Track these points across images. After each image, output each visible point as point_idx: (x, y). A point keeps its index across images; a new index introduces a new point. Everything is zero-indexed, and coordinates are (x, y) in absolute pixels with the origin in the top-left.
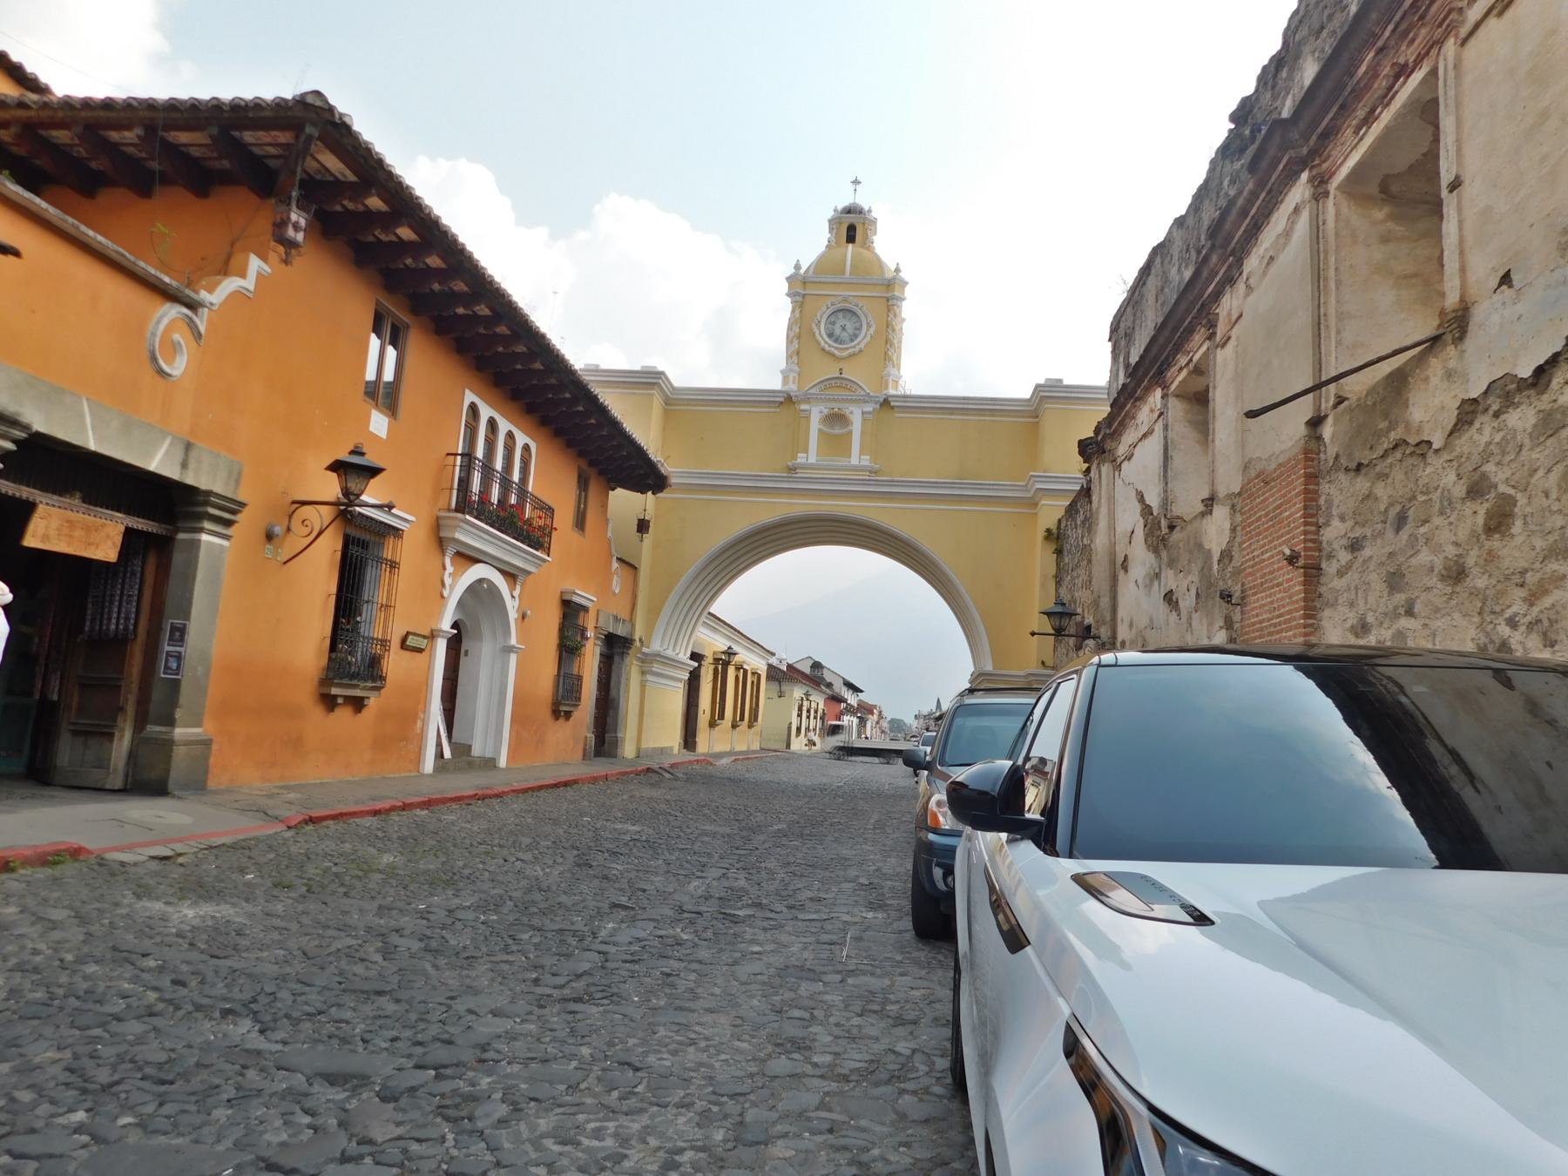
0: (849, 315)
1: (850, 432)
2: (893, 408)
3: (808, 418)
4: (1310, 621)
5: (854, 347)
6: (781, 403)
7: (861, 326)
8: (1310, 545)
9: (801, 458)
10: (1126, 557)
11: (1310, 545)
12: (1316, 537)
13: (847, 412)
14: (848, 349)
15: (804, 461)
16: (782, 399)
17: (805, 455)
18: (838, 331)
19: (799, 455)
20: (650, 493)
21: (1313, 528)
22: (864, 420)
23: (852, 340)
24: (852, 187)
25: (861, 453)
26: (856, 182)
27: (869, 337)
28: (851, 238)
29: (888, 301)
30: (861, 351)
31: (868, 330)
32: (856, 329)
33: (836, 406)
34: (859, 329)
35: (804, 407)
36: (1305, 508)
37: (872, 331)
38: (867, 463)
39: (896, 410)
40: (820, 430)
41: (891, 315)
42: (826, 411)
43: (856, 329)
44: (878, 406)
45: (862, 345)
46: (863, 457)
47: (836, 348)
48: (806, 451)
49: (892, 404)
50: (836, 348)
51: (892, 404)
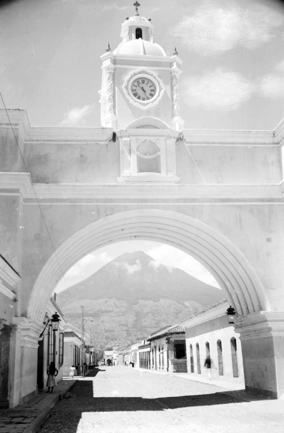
7: (155, 88)
18: (140, 92)
24: (135, 7)
26: (137, 4)
31: (160, 91)
32: (152, 91)
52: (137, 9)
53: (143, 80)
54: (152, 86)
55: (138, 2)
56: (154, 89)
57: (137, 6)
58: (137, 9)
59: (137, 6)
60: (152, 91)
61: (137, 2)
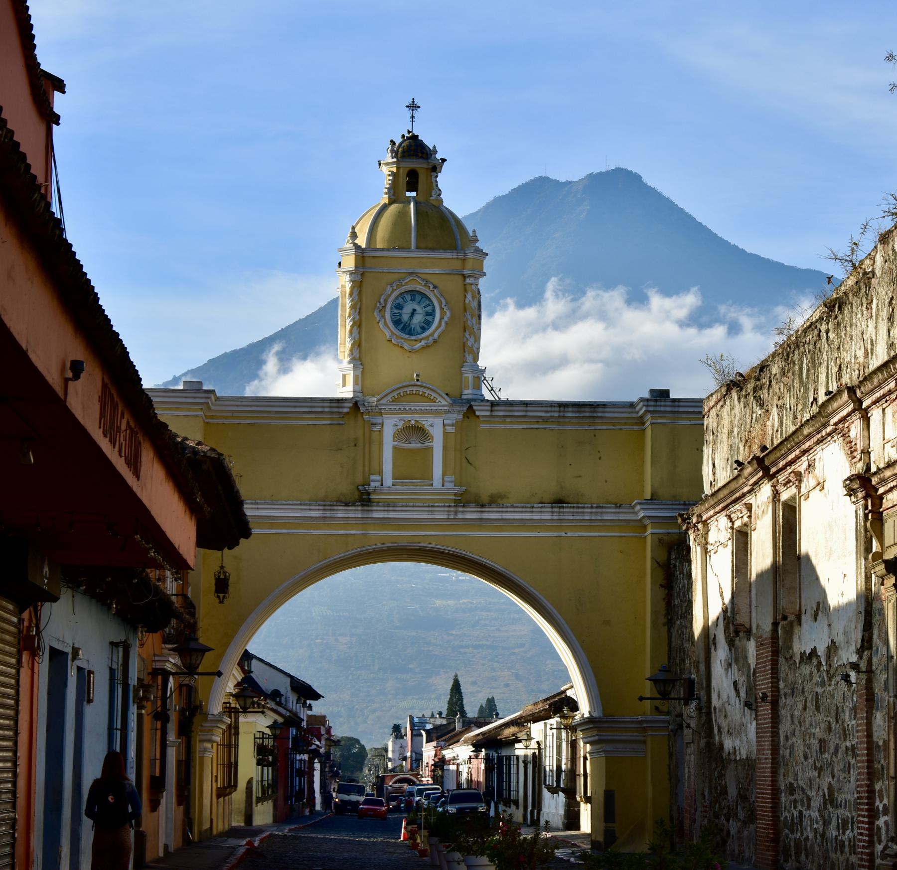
0: (418, 297)
1: (431, 448)
2: (478, 416)
3: (381, 432)
4: (775, 730)
5: (427, 338)
6: (347, 413)
7: (434, 310)
8: (774, 689)
10: (715, 635)
11: (774, 689)
12: (777, 685)
13: (426, 425)
14: (421, 340)
15: (378, 484)
16: (346, 410)
17: (378, 478)
20: (226, 548)
21: (776, 680)
22: (446, 434)
23: (424, 329)
24: (408, 113)
26: (413, 106)
28: (412, 185)
30: (435, 342)
31: (441, 318)
33: (413, 418)
34: (432, 314)
36: (772, 669)
39: (482, 419)
40: (395, 448)
41: (469, 296)
42: (401, 424)
43: (427, 314)
44: (461, 416)
45: (436, 335)
48: (380, 473)
49: (477, 413)
51: (477, 413)
52: (413, 117)
53: (414, 294)
54: (429, 305)
56: (430, 311)
57: (413, 110)
58: (413, 117)
59: (413, 110)
60: (427, 314)
61: (413, 102)
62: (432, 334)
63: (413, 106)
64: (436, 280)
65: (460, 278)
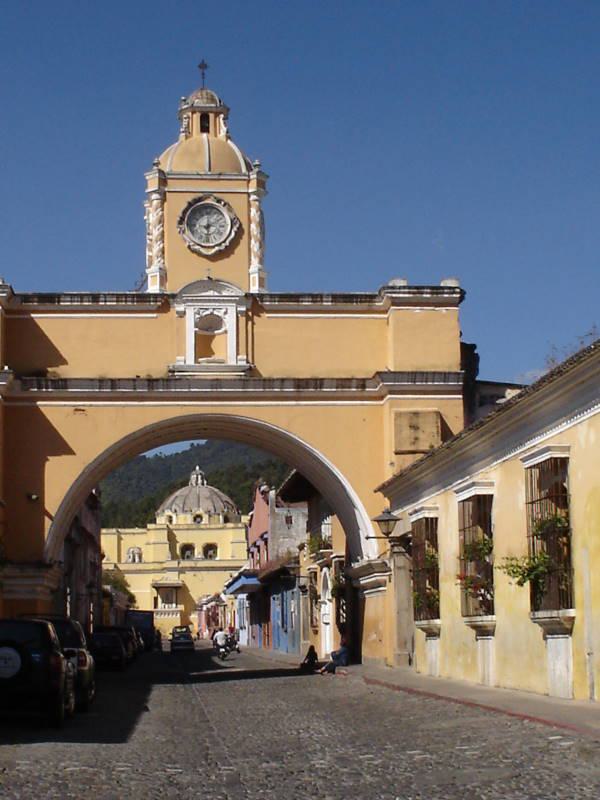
5: (220, 245)
9: (179, 362)
15: (182, 363)
19: (179, 358)
24: (200, 71)
25: (238, 354)
26: (203, 66)
27: (233, 234)
29: (249, 196)
35: (180, 308)
37: (235, 229)
38: (244, 363)
40: (196, 332)
46: (239, 357)
47: (202, 247)
48: (182, 352)
50: (202, 247)
52: (203, 74)
55: (205, 62)
58: (203, 74)
62: (224, 242)
63: (203, 66)
64: (226, 198)
65: (246, 196)
